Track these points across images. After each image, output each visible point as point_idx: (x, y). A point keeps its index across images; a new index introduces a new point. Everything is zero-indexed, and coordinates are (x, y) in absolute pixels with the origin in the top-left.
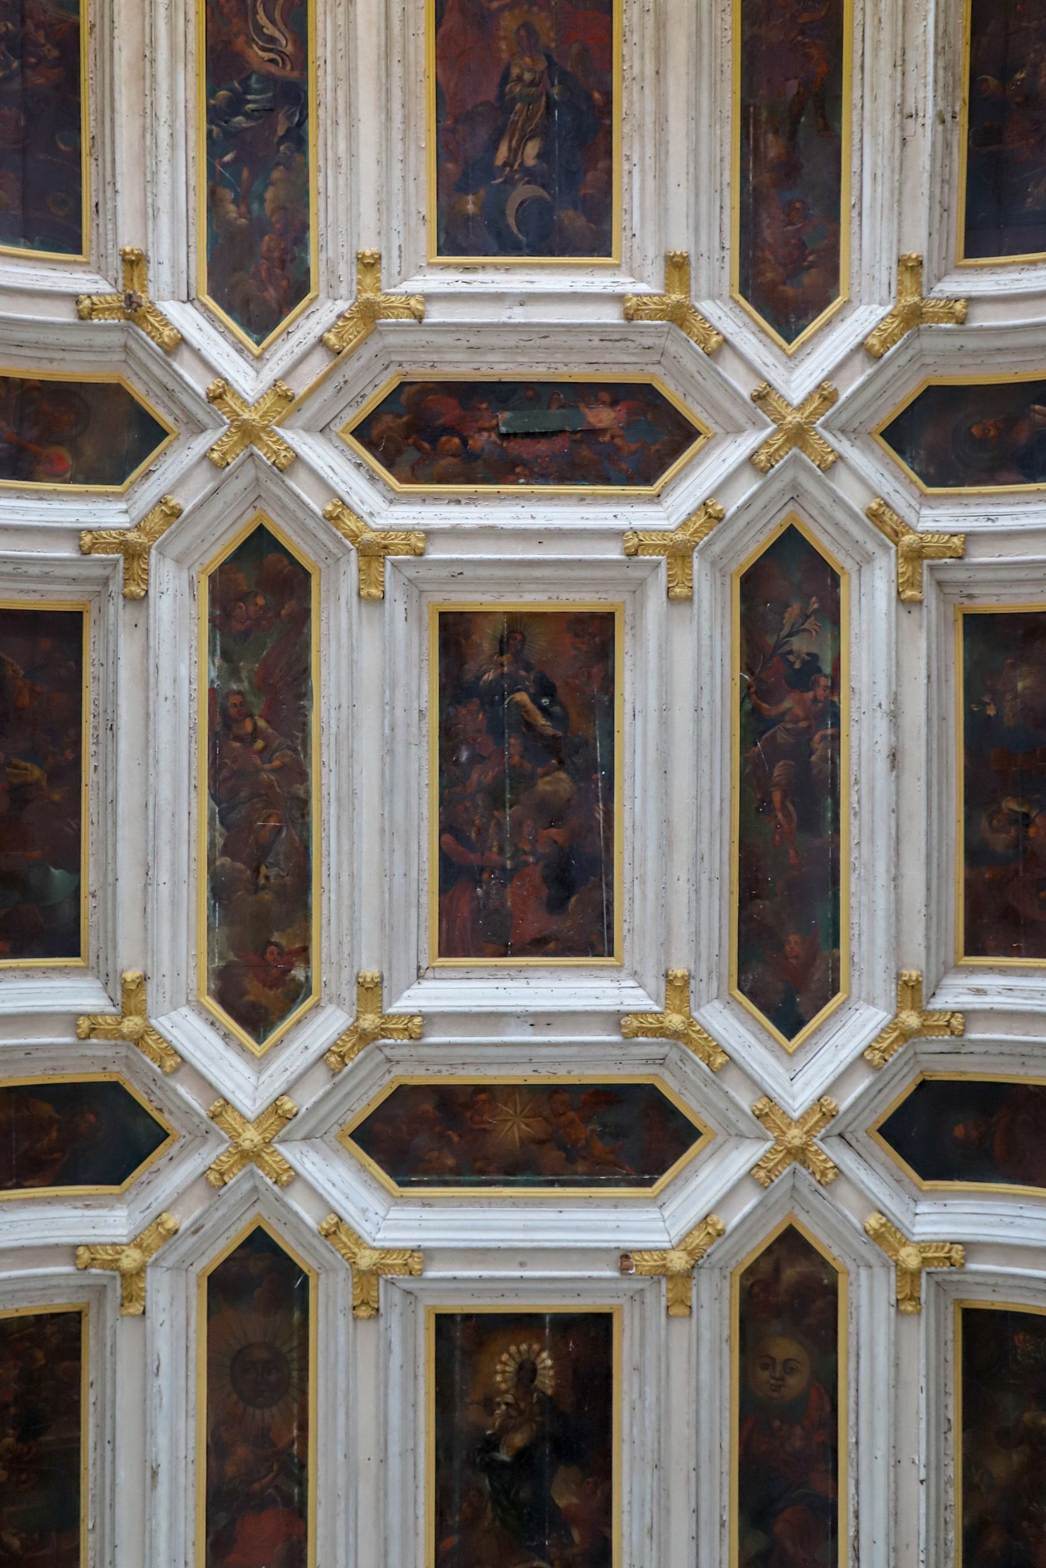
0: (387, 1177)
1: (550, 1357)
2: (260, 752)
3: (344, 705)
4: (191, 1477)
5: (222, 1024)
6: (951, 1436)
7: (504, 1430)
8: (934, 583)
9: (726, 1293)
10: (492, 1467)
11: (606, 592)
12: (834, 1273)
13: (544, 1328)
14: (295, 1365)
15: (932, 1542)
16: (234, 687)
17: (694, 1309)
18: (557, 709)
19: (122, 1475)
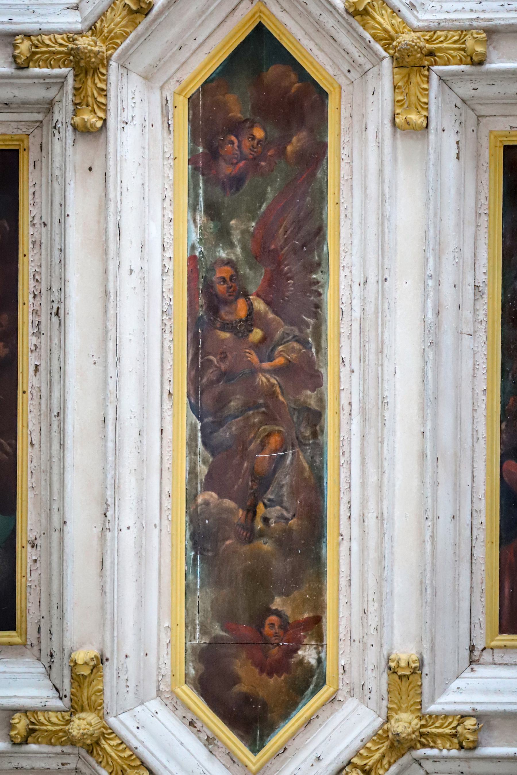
2: (257, 346)
3: (372, 279)
5: (204, 724)
16: (223, 254)
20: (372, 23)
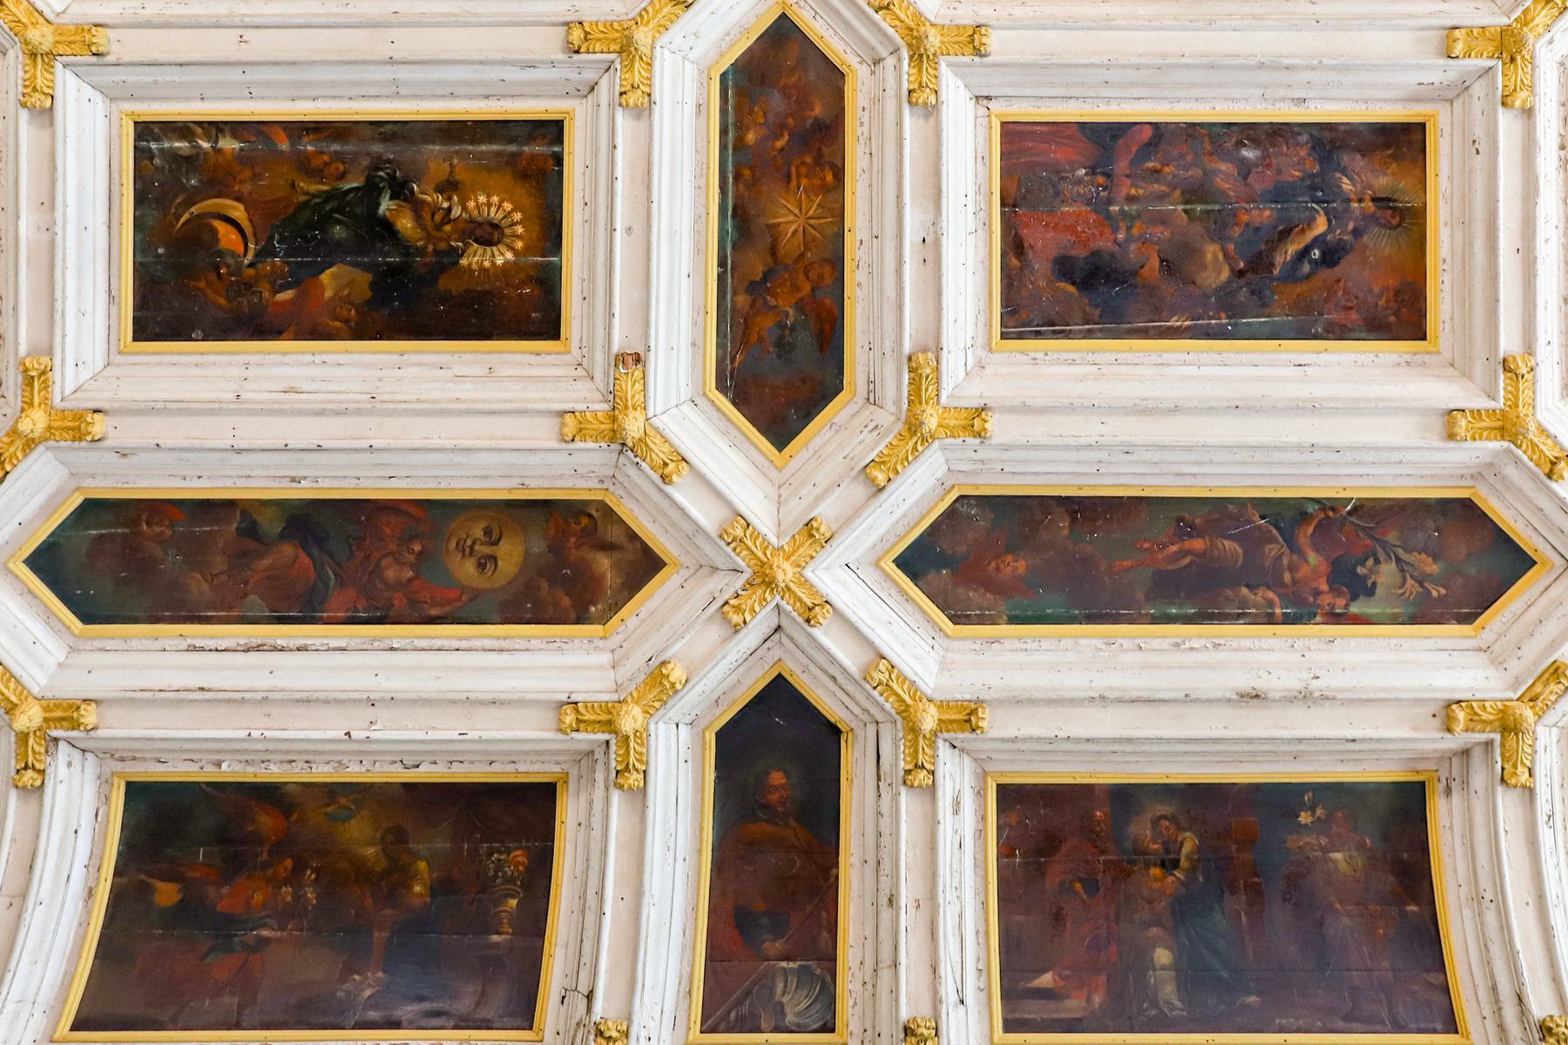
1: (507, 263)
6: (398, 768)
7: (417, 207)
8: (1468, 746)
10: (371, 191)
11: (1453, 330)
12: (603, 619)
13: (543, 256)
15: (271, 746)
18: (1306, 268)
20: (1539, 7)
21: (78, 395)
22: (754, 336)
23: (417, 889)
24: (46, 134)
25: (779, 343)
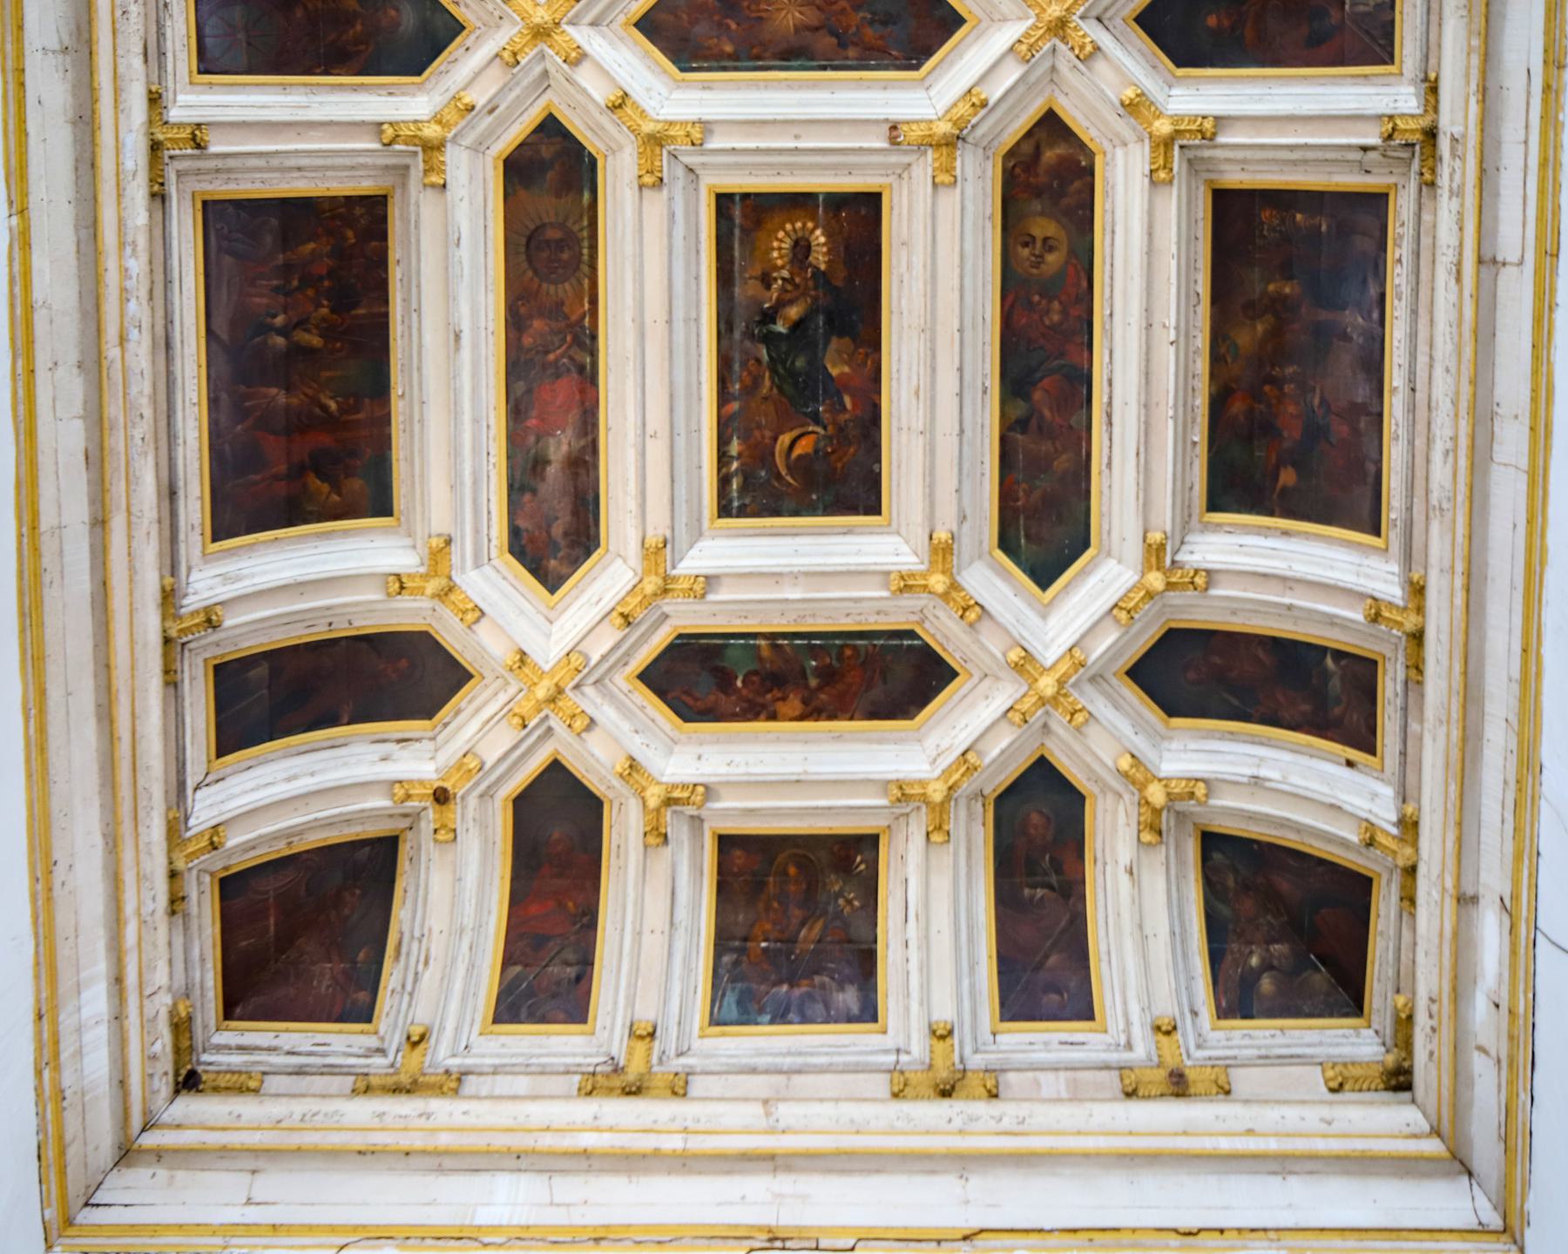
0: (670, 64)
1: (823, 234)
4: (491, 348)
6: (1200, 309)
7: (781, 304)
9: (989, 173)
10: (770, 339)
12: (1091, 155)
14: (586, 243)
15: (1181, 403)
17: (959, 179)
19: (428, 338)
21: (920, 553)
22: (880, 42)
23: (1287, 290)
24: (725, 581)
25: (884, 23)
